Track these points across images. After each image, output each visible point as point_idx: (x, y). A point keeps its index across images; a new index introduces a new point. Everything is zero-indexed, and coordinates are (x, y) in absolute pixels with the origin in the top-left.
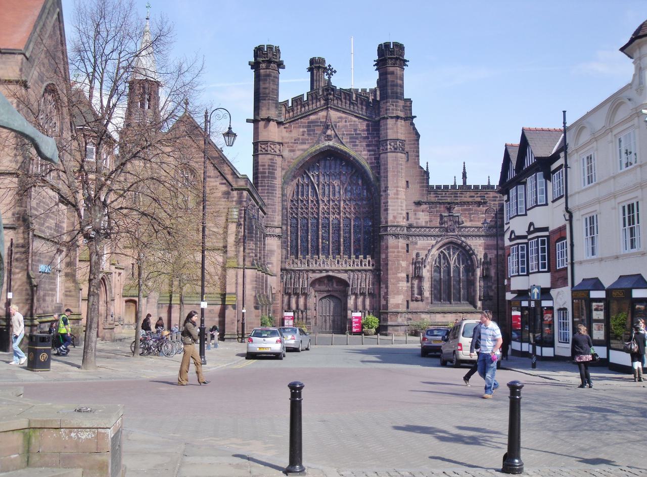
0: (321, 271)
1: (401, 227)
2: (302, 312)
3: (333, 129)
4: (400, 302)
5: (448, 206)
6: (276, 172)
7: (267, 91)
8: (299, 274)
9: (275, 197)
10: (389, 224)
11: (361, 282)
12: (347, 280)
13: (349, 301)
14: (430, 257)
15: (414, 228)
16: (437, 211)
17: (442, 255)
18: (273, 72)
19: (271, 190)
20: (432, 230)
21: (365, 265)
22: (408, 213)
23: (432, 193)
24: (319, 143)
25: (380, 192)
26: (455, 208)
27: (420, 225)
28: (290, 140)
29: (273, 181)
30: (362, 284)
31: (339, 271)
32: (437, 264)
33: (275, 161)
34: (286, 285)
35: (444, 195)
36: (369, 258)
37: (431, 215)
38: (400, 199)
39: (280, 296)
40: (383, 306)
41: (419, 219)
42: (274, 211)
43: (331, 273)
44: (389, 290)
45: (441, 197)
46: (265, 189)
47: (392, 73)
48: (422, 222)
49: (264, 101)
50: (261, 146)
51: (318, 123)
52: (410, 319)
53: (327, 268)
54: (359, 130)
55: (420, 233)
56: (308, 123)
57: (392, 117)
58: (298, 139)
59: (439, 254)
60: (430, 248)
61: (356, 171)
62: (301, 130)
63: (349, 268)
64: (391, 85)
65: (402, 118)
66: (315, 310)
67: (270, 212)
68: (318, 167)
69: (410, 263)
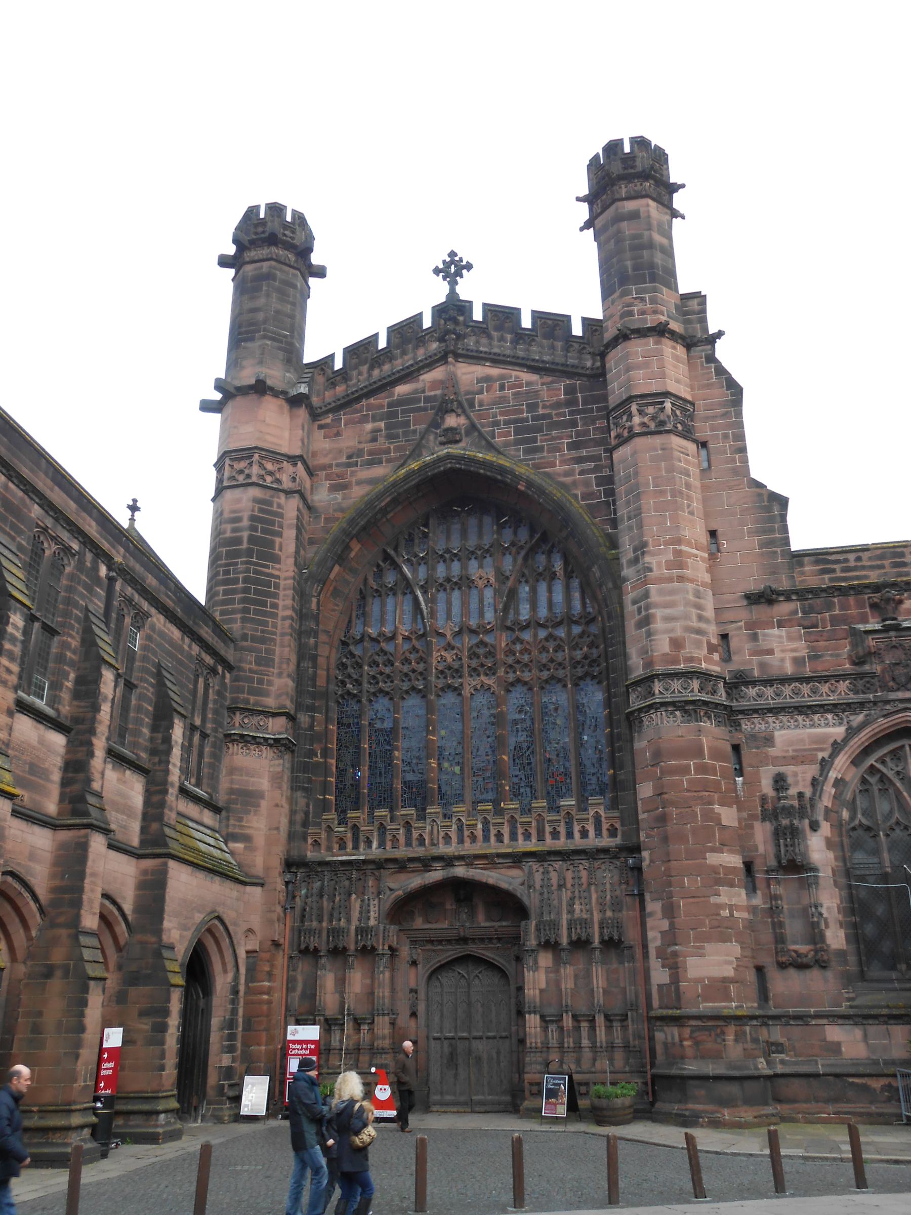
0: (426, 863)
1: (705, 677)
2: (358, 1023)
3: (464, 412)
4: (729, 972)
5: (876, 598)
6: (278, 540)
7: (260, 316)
8: (350, 879)
9: (274, 615)
10: (659, 668)
11: (572, 899)
12: (521, 892)
13: (529, 975)
14: (829, 790)
15: (754, 683)
16: (834, 620)
17: (873, 780)
18: (281, 270)
19: (257, 592)
20: (825, 688)
21: (584, 834)
22: (724, 637)
23: (806, 559)
24: (420, 455)
25: (620, 567)
26: (901, 602)
27: (774, 673)
28: (336, 459)
29: (267, 567)
30: (577, 907)
31: (490, 860)
32: (859, 816)
33: (275, 508)
34: (303, 916)
35: (852, 564)
36: (598, 807)
37: (813, 638)
38: (691, 581)
39: (281, 960)
40: (661, 998)
41: (770, 652)
42: (265, 661)
43: (460, 871)
44: (682, 919)
45: (844, 570)
46: (234, 592)
47: (634, 216)
48: (782, 660)
49: (249, 344)
50: (232, 466)
51: (420, 402)
52: (778, 1048)
53: (443, 849)
54: (544, 407)
55: (780, 700)
56: (390, 405)
57: (642, 333)
58: (360, 453)
59: (864, 781)
60: (826, 754)
61: (544, 538)
62: (369, 426)
63: (523, 846)
64: (634, 248)
65: (673, 335)
66: (414, 1014)
67: (249, 663)
68: (426, 535)
69: (753, 817)
